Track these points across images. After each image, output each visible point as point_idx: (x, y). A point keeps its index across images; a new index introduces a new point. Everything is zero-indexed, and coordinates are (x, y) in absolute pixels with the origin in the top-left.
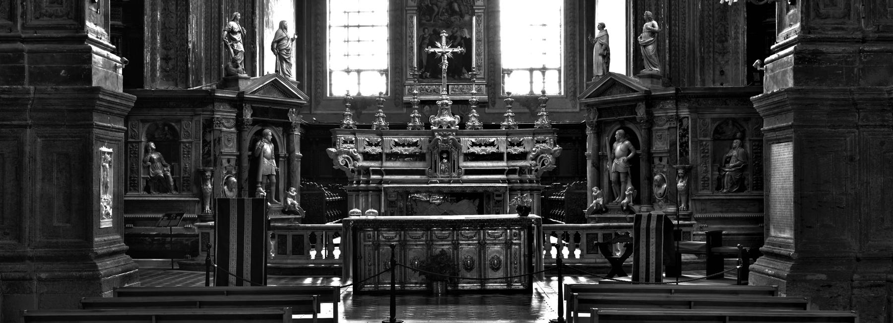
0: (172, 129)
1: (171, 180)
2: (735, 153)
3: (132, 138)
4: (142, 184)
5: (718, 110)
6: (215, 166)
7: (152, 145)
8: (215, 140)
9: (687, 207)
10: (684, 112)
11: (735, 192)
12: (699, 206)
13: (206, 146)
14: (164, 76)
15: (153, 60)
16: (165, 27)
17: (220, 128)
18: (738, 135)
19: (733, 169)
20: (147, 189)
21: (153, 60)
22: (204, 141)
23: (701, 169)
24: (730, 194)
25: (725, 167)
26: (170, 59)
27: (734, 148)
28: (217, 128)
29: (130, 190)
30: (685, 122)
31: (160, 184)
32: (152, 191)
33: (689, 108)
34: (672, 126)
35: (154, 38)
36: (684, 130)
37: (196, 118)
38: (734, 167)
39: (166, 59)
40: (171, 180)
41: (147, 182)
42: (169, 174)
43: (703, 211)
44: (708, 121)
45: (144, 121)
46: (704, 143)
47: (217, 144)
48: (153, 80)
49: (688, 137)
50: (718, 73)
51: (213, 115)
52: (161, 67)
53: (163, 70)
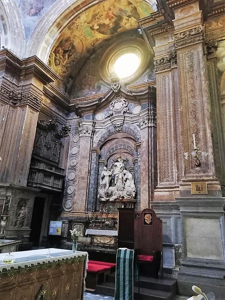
2: (22, 212)
5: (21, 195)
9: (3, 233)
10: (9, 194)
11: (21, 227)
12: (9, 233)
18: (24, 205)
19: (21, 218)
23: (11, 217)
24: (19, 228)
25: (18, 217)
27: (22, 210)
30: (9, 198)
33: (12, 193)
34: (3, 198)
36: (8, 201)
38: (21, 217)
43: (10, 235)
44: (17, 198)
46: (14, 207)
49: (9, 204)
50: (18, 181)
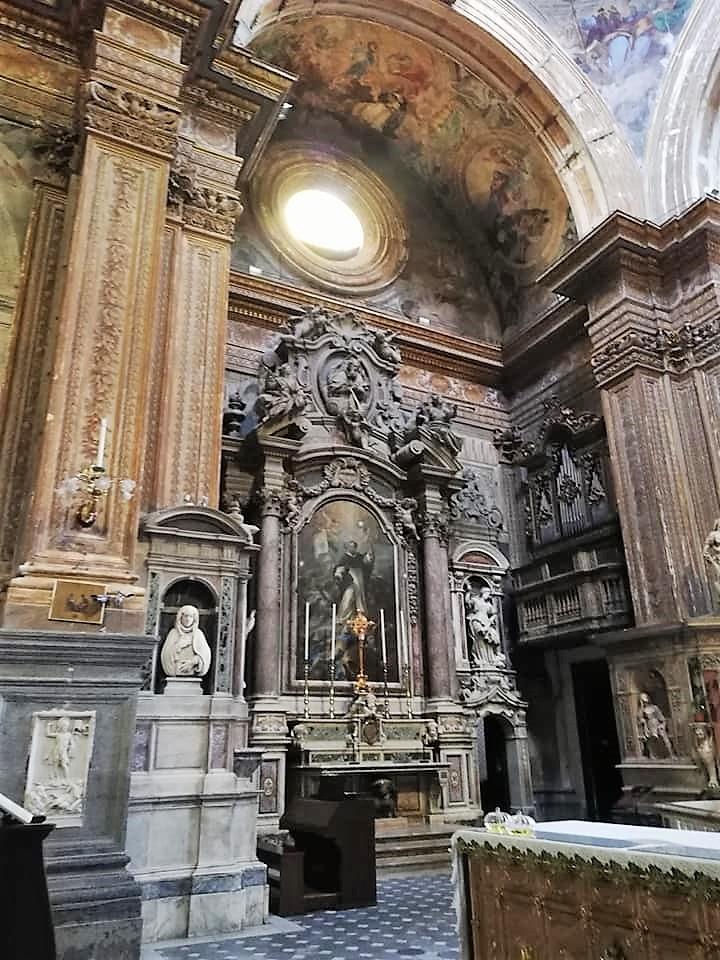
0: (656, 673)
1: (667, 741)
3: (621, 690)
4: (640, 748)
6: (715, 720)
7: (644, 697)
8: (707, 685)
13: (698, 693)
14: (655, 612)
15: (641, 596)
16: (647, 558)
17: (714, 668)
20: (646, 753)
21: (641, 596)
22: (694, 687)
26: (657, 591)
28: (709, 668)
29: (629, 756)
31: (654, 746)
32: (651, 755)
35: (638, 571)
37: (680, 658)
39: (653, 593)
40: (667, 741)
41: (645, 744)
42: (663, 733)
45: (629, 668)
47: (712, 690)
48: (645, 620)
51: (698, 651)
52: (650, 602)
53: (654, 606)
